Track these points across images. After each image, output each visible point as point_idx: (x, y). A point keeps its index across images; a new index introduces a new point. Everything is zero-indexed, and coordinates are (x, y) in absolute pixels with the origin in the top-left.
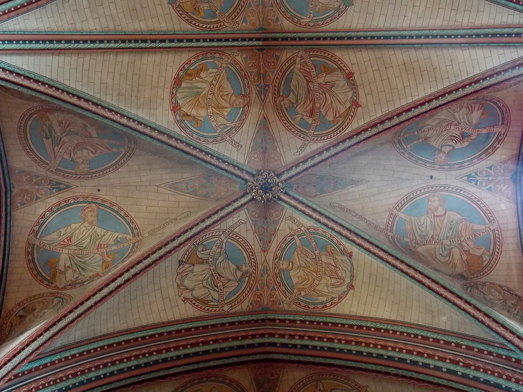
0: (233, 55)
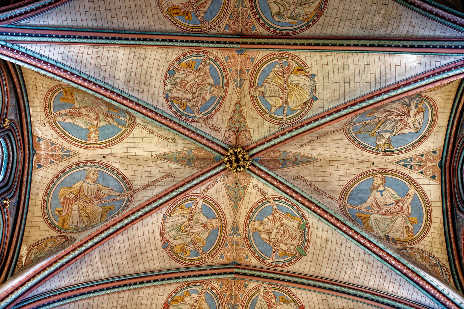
0: (211, 283)
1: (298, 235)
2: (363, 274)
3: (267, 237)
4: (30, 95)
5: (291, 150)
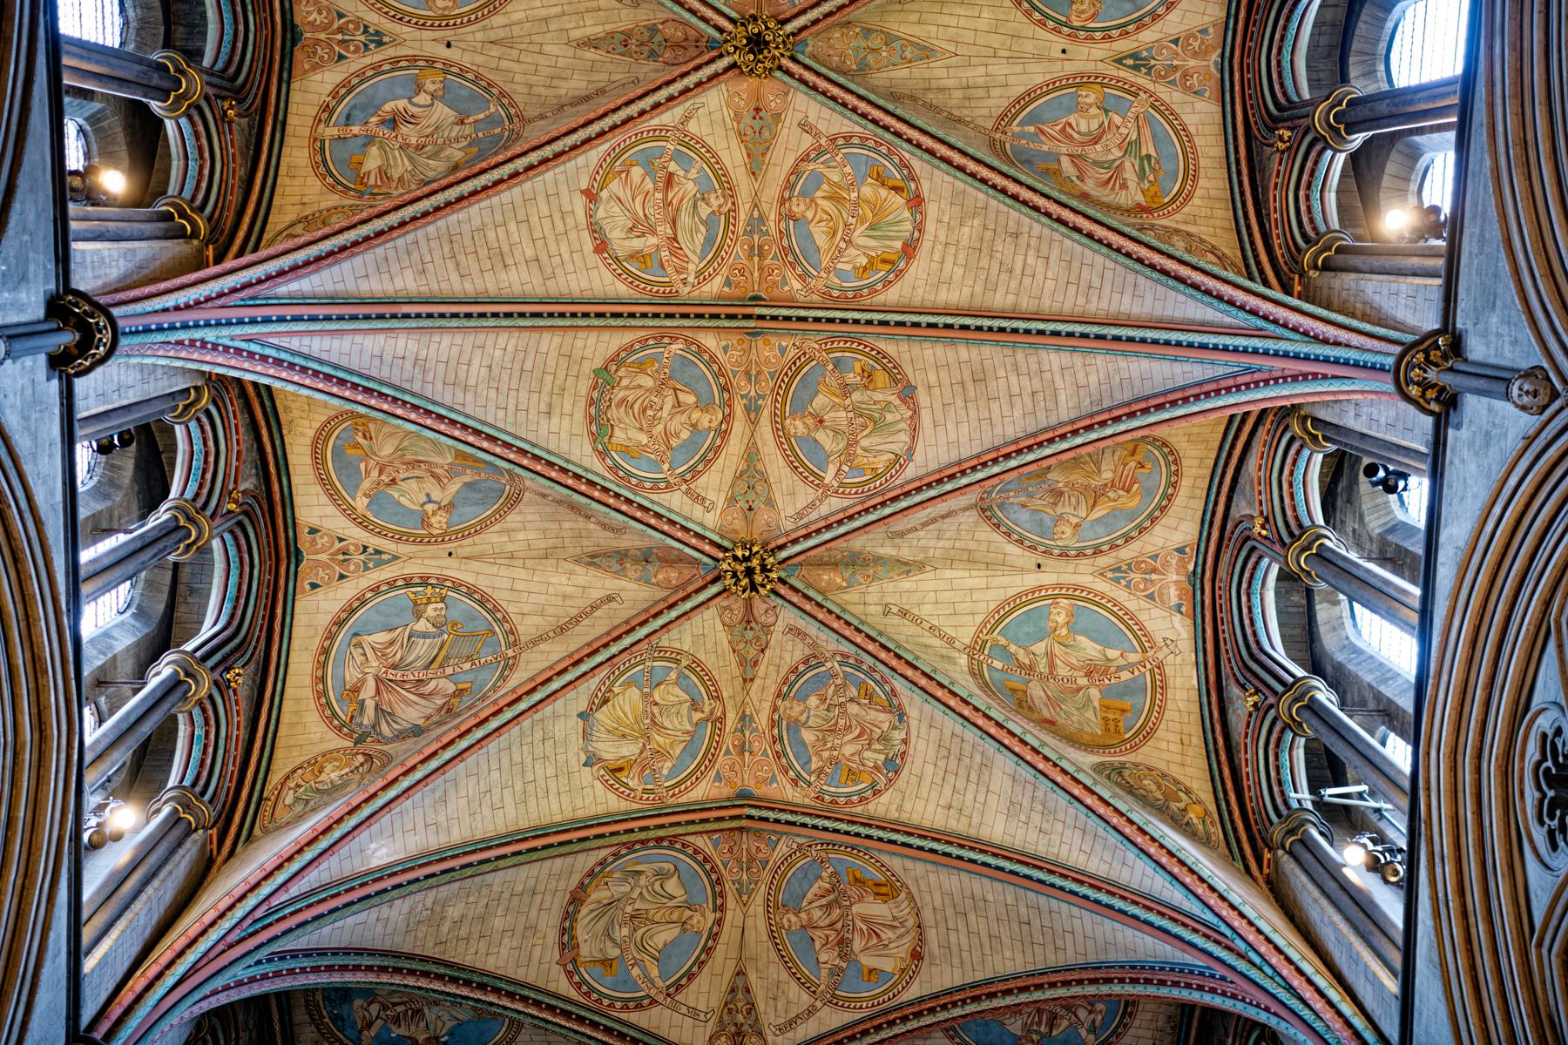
1: (613, 413)
2: (465, 359)
3: (682, 396)
4: (1196, 717)
5: (632, 586)
